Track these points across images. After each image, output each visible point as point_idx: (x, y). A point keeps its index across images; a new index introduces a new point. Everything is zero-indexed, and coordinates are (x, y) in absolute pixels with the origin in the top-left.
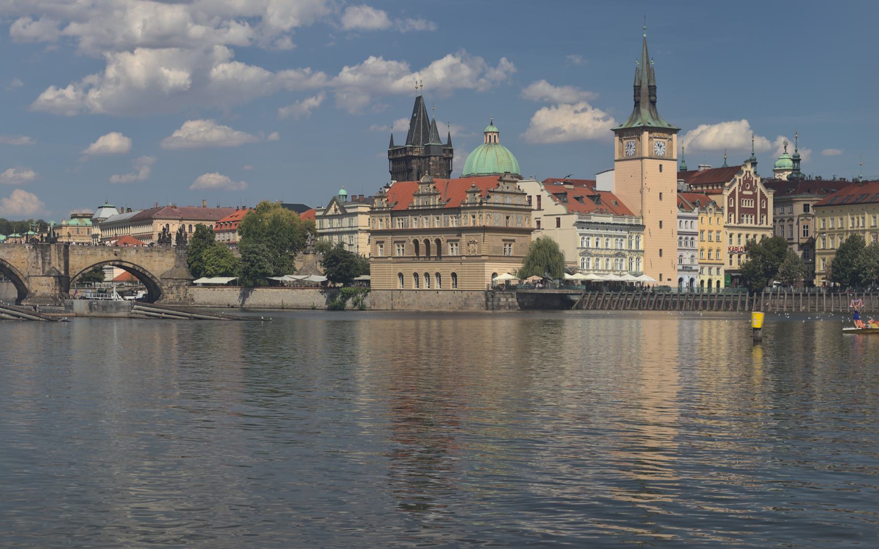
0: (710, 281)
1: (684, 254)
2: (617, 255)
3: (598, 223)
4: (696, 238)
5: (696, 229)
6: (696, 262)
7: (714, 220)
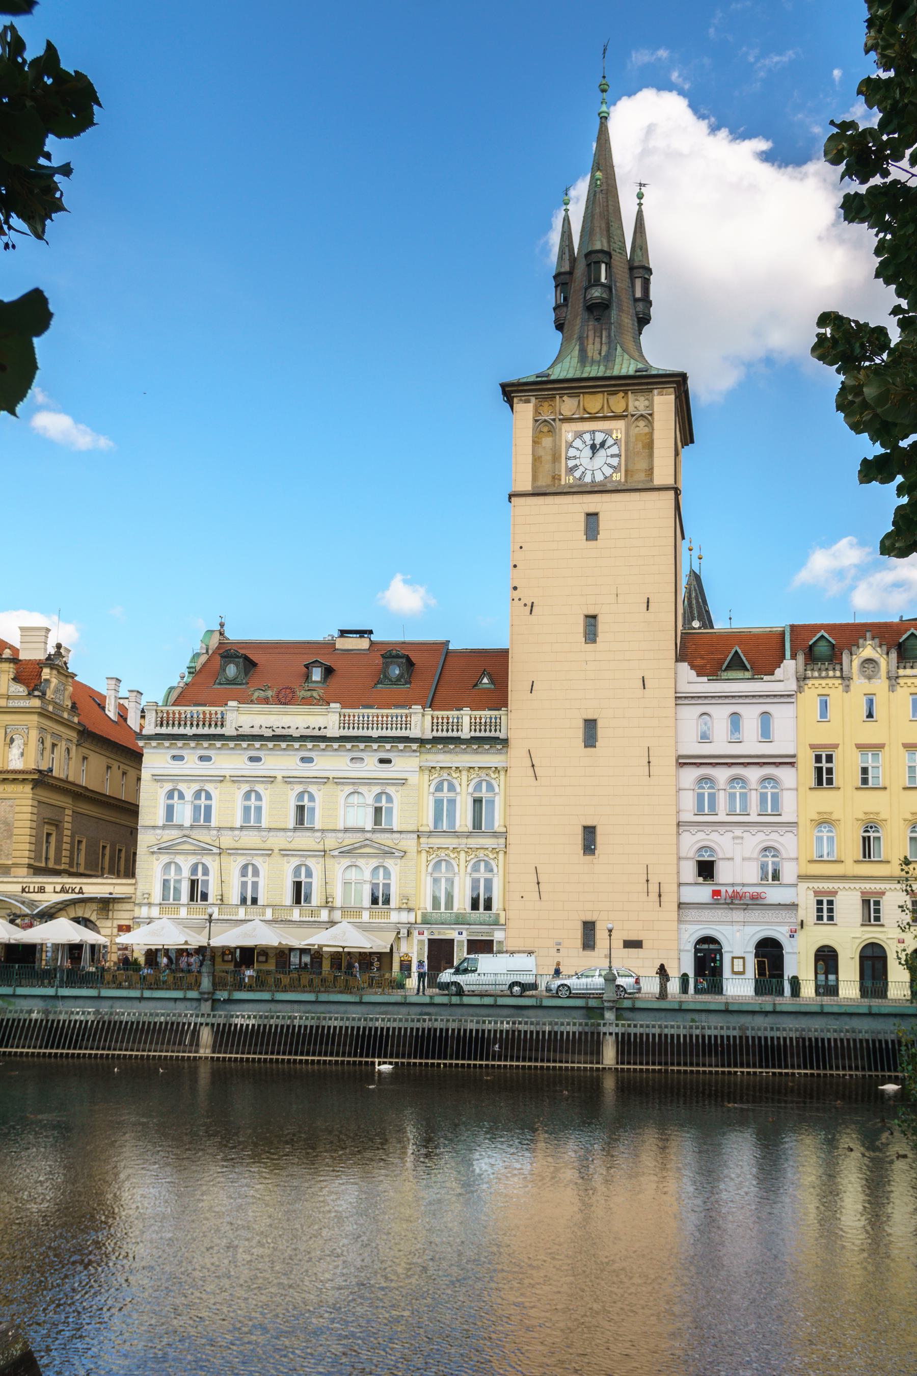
3: (260, 738)
4: (785, 775)
5: (780, 746)
6: (789, 873)
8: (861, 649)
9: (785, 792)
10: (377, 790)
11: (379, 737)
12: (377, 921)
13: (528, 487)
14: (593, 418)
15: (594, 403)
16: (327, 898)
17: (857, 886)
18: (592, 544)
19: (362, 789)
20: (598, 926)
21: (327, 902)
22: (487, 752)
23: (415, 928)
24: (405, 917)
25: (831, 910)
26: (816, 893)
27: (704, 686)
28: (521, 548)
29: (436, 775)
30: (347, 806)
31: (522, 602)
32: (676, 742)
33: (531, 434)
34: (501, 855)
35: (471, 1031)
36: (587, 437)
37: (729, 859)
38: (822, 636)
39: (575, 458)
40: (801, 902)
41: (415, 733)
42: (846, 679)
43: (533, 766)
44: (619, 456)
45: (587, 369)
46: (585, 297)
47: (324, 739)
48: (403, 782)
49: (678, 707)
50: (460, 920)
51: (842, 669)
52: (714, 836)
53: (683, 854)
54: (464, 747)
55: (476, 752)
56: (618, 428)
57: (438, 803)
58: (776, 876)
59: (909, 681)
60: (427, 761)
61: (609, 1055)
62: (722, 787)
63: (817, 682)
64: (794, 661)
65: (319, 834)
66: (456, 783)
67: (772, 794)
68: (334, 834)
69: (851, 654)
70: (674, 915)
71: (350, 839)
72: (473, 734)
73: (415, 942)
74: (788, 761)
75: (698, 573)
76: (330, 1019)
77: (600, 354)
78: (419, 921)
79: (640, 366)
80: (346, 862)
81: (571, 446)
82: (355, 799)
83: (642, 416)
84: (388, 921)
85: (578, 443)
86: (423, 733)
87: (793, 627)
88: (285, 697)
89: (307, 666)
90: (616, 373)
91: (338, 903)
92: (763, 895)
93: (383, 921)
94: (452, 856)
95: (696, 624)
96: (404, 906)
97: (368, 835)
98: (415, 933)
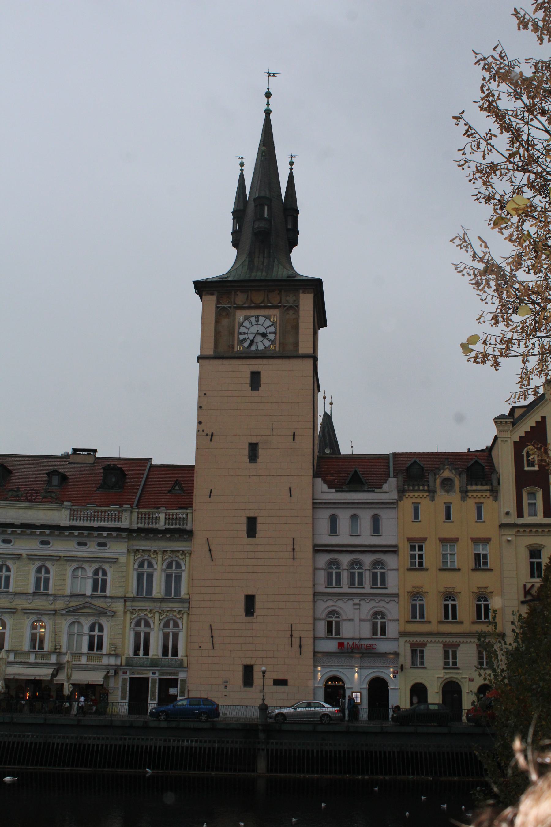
0: (451, 690)
1: (346, 608)
2: (73, 611)
6: (392, 630)
7: (464, 510)
8: (442, 471)
9: (390, 572)
10: (95, 566)
11: (99, 527)
12: (92, 663)
13: (210, 352)
14: (258, 307)
15: (258, 298)
16: (56, 646)
17: (440, 640)
18: (256, 393)
19: (86, 566)
20: (256, 669)
21: (56, 649)
22: (177, 540)
23: (121, 669)
24: (112, 661)
25: (422, 657)
26: (412, 645)
27: (333, 495)
28: (205, 394)
29: (139, 556)
30: (74, 578)
31: (205, 432)
32: (313, 535)
33: (213, 315)
34: (185, 616)
35: (160, 747)
36: (253, 319)
37: (350, 620)
38: (415, 462)
39: (244, 333)
40: (402, 652)
41: (125, 524)
42: (432, 493)
43: (210, 550)
44: (274, 333)
45: (254, 274)
46: (253, 227)
47: (57, 527)
48: (114, 561)
49: (315, 510)
50: (155, 663)
51: (429, 485)
52: (340, 603)
53: (318, 615)
54: (160, 536)
55: (170, 540)
56: (275, 315)
57: (140, 576)
58: (383, 632)
59: (475, 494)
60: (133, 545)
61: (262, 766)
62: (345, 567)
63: (411, 494)
64: (395, 479)
65: (51, 598)
66: (154, 562)
67: (381, 573)
68: (63, 598)
69: (435, 475)
70: (311, 661)
71: (74, 603)
72: (167, 526)
73: (120, 680)
74: (393, 550)
75: (329, 414)
76: (54, 737)
77: (263, 264)
78: (124, 663)
79: (290, 273)
80: (71, 619)
81: (242, 325)
82: (80, 572)
83: (291, 307)
84: (101, 663)
85: (247, 323)
86: (131, 524)
87: (395, 455)
88: (31, 497)
89: (48, 474)
90: (274, 277)
91: (64, 650)
92: (374, 646)
93: (97, 663)
94: (150, 616)
95: (327, 451)
96: (113, 652)
97: (88, 600)
98: (121, 673)
